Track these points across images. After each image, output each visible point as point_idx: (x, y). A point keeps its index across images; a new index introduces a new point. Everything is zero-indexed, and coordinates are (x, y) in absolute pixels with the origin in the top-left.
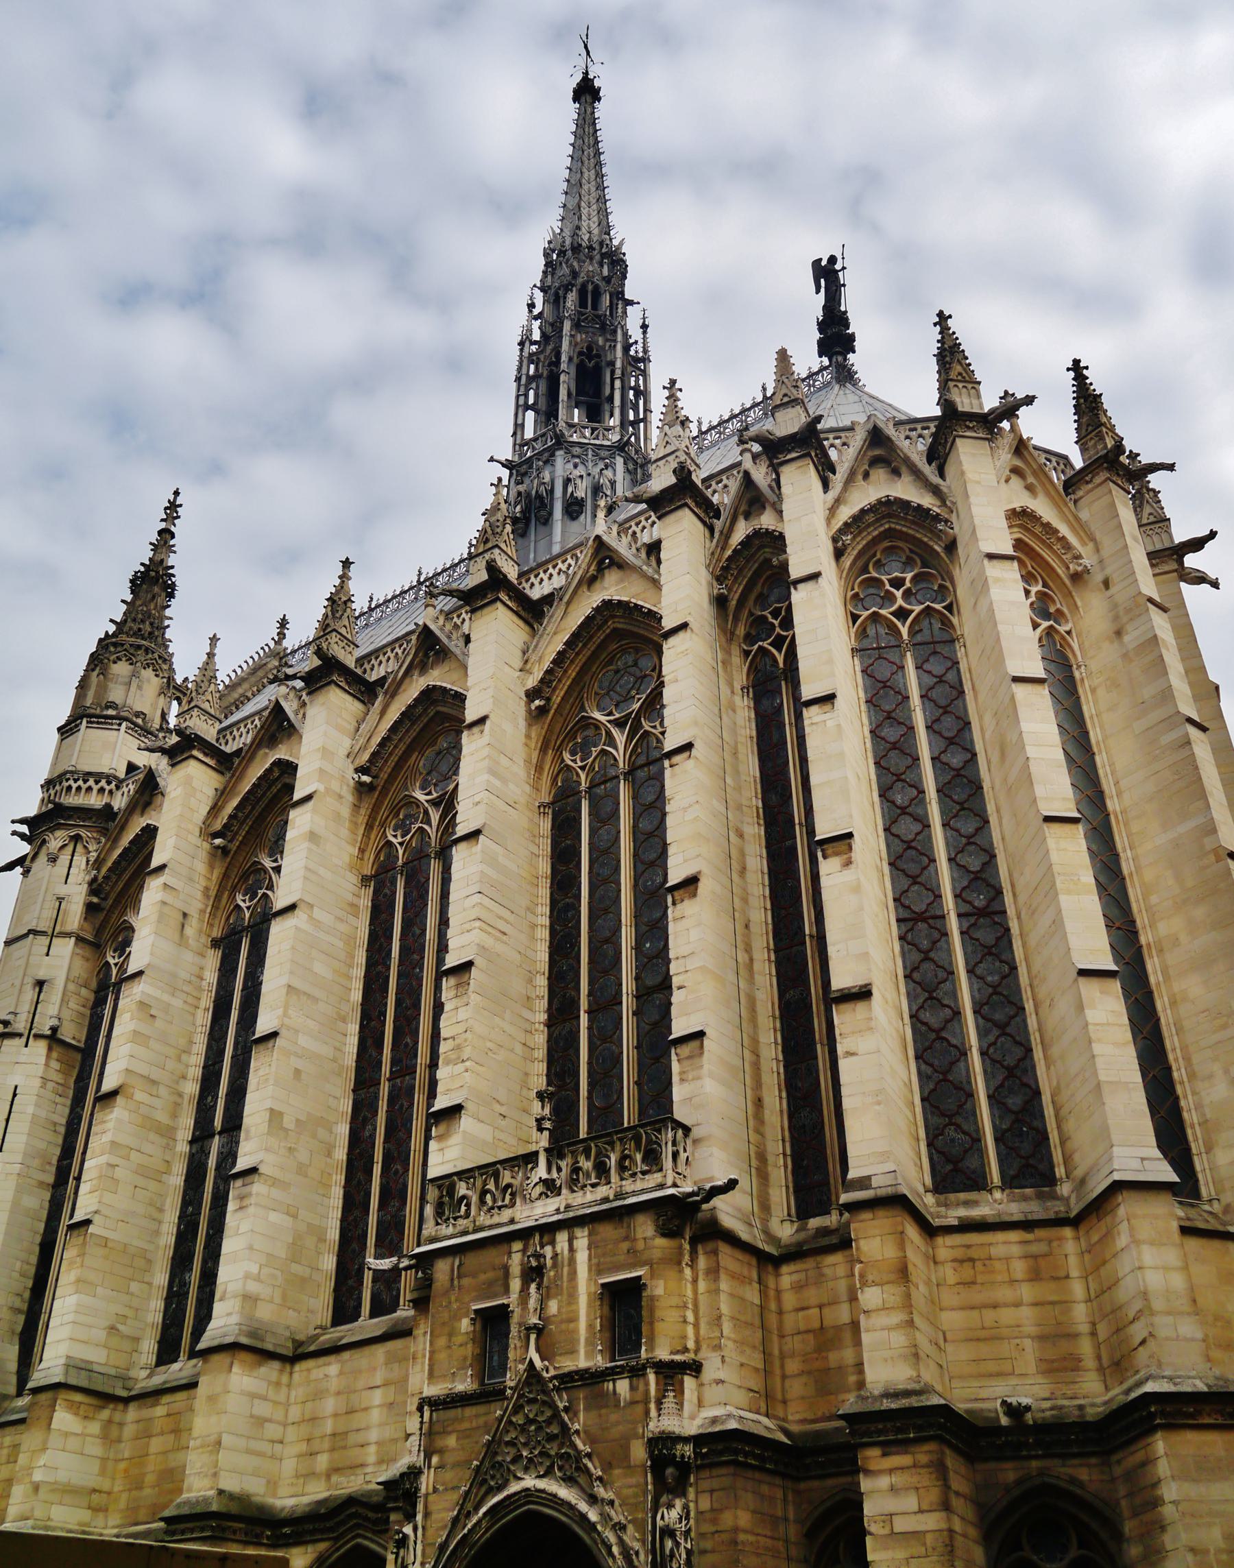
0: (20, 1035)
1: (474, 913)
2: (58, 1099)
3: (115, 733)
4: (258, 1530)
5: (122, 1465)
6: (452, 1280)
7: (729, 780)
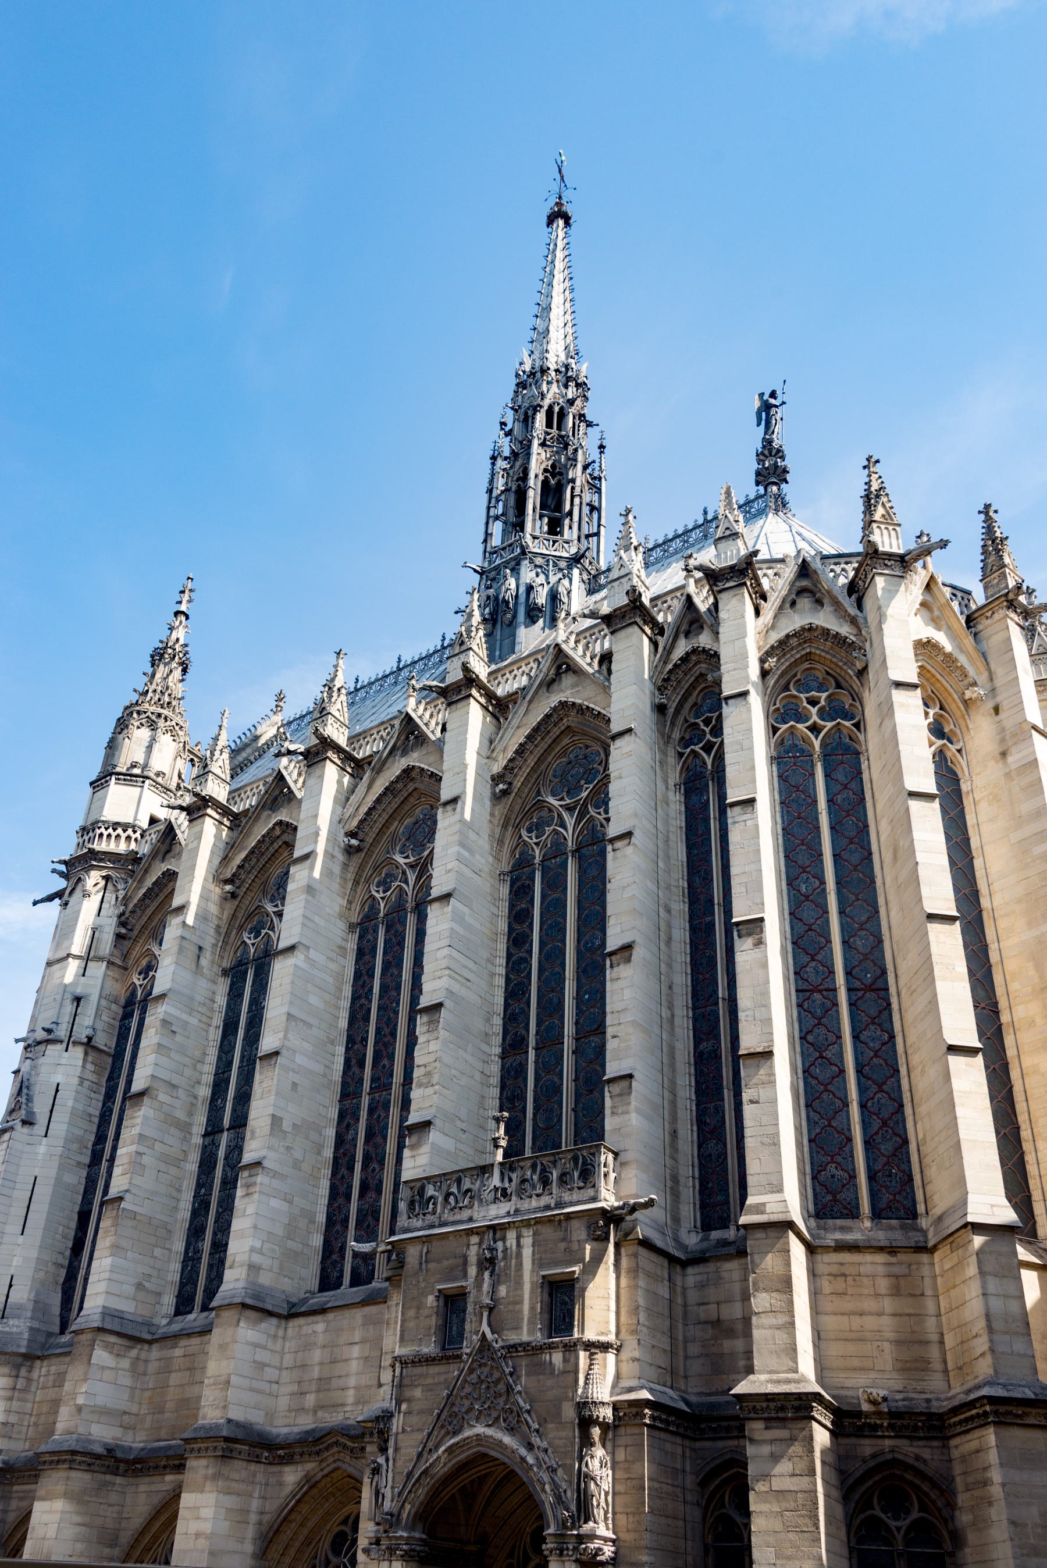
0: (61, 1042)
1: (444, 963)
2: (93, 1095)
4: (258, 1451)
5: (148, 1394)
6: (421, 1264)
7: (661, 864)
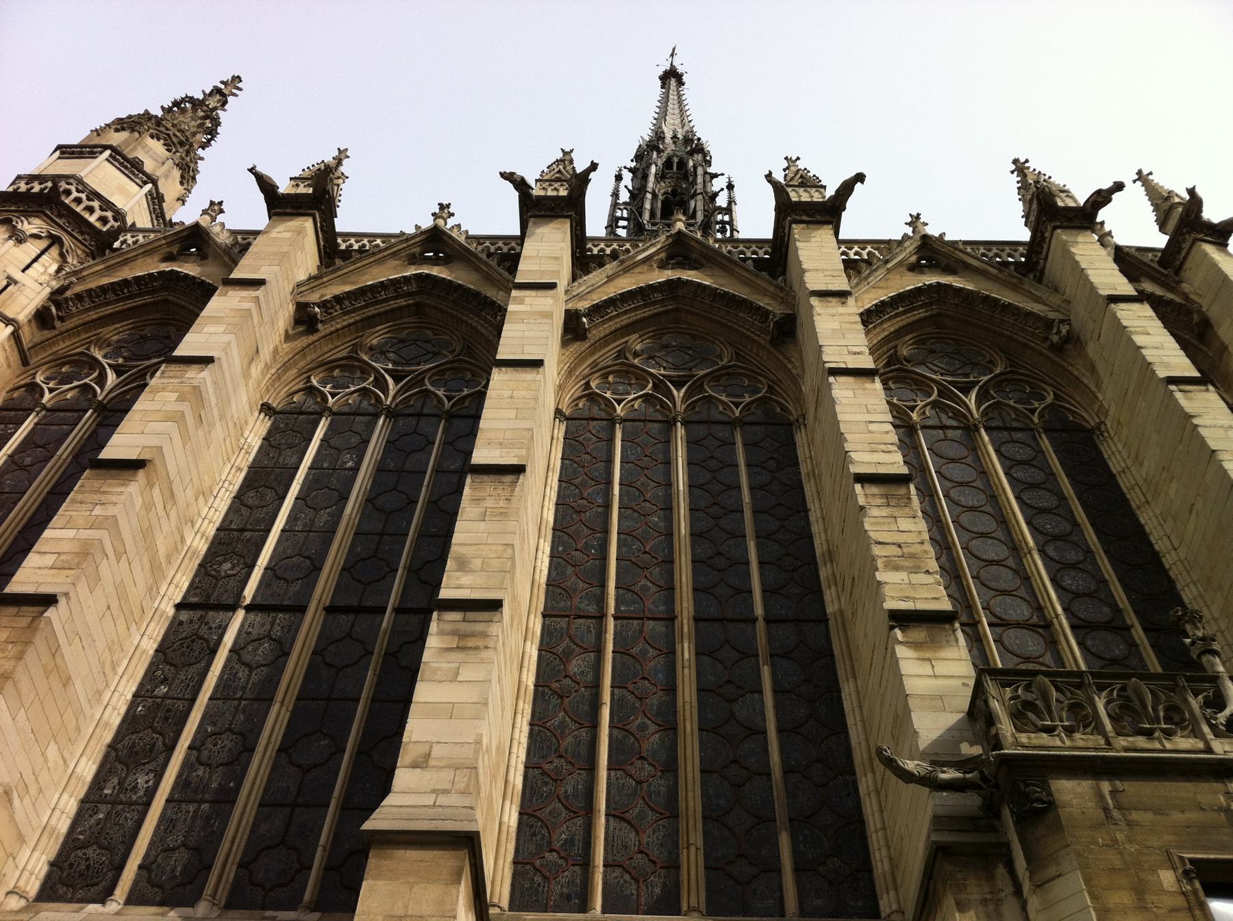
3: (137, 188)
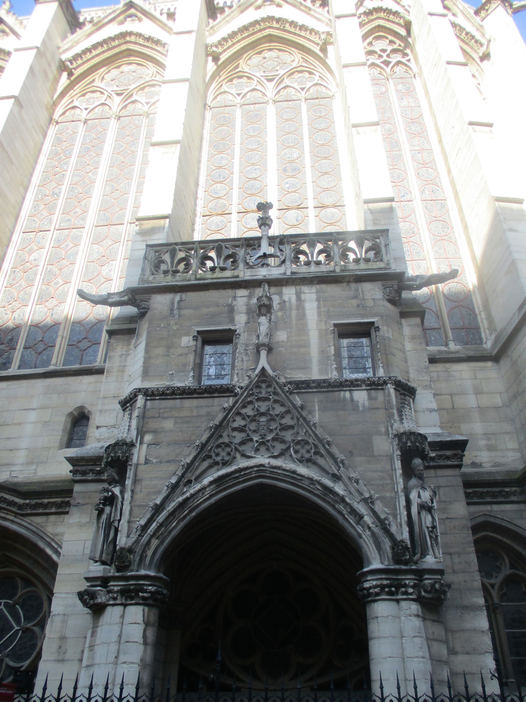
6: (172, 310)
